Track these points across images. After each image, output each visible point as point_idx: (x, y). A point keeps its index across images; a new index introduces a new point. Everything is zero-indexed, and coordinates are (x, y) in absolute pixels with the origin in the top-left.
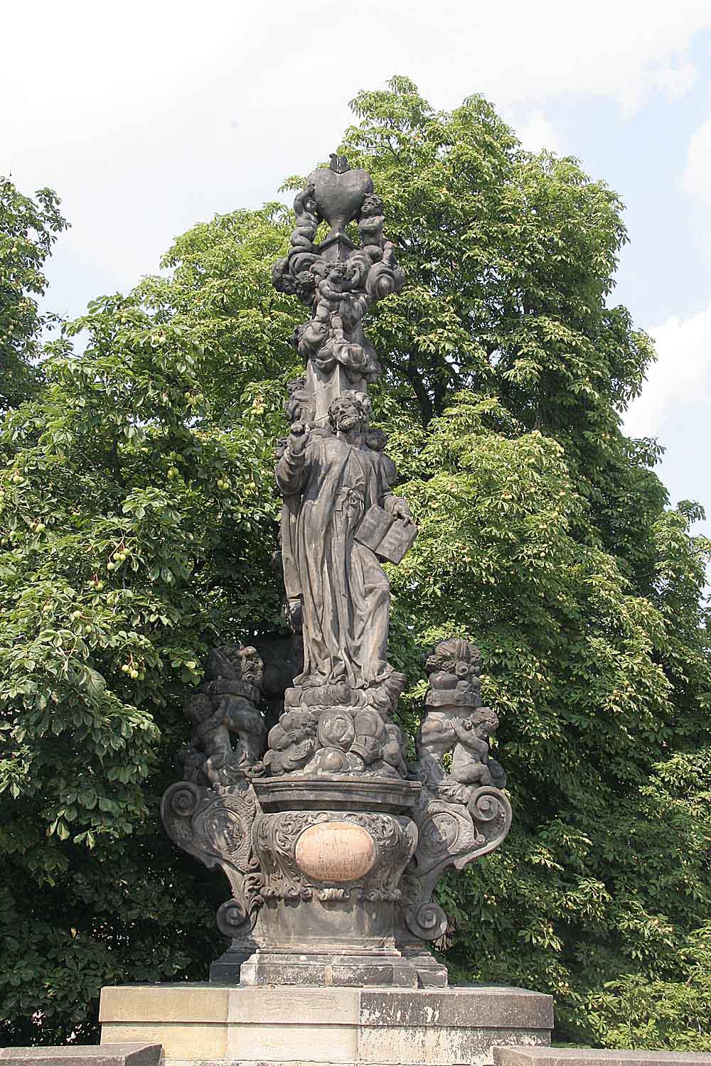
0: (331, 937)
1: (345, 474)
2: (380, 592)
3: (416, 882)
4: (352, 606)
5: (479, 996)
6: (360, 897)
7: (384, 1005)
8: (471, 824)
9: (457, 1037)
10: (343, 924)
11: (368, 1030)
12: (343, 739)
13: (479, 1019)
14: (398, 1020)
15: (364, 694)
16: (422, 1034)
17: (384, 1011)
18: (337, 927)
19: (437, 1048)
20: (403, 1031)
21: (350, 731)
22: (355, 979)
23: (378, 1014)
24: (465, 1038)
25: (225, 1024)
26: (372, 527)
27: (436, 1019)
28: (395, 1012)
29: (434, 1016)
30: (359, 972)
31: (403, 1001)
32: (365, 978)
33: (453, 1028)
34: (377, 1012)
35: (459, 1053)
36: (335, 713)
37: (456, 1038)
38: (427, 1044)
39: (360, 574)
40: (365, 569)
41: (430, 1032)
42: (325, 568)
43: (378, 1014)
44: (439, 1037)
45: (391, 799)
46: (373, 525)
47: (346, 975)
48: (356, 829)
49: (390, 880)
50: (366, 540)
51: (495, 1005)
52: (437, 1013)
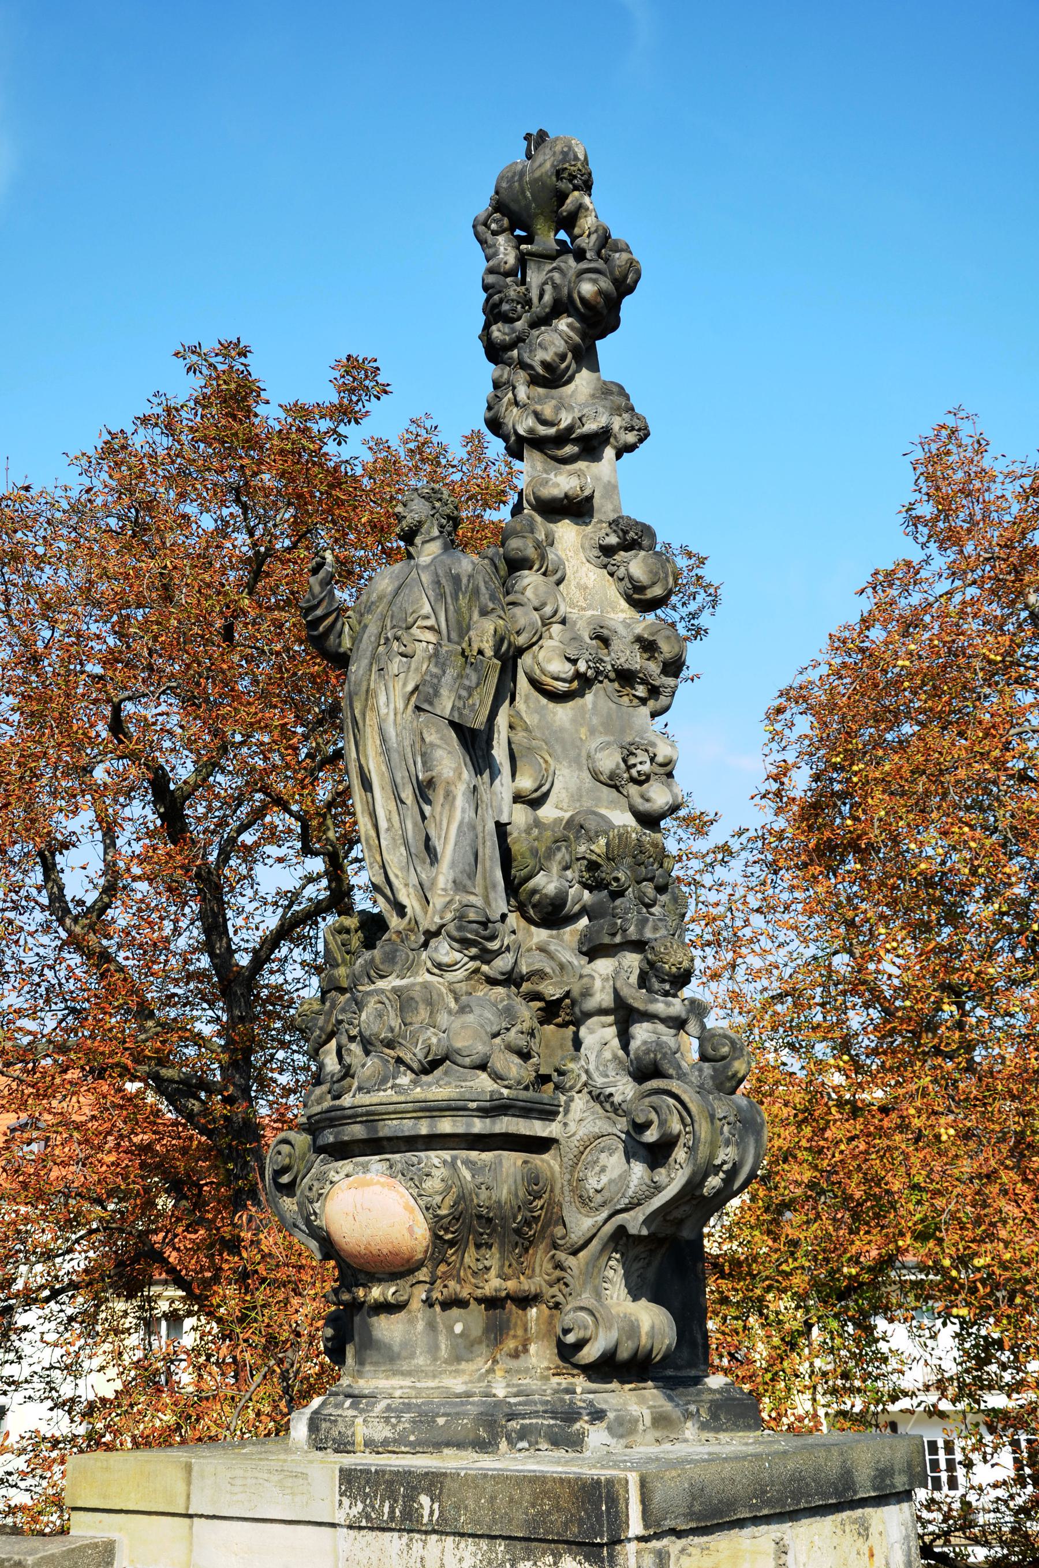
0: (388, 1367)
10: (404, 1344)
13: (494, 1521)
16: (421, 1544)
22: (395, 1441)
24: (479, 1557)
25: (191, 1516)
26: (435, 681)
28: (382, 1502)
32: (412, 1438)
33: (462, 1535)
37: (467, 1555)
48: (382, 1185)
50: (431, 703)
52: (436, 1506)
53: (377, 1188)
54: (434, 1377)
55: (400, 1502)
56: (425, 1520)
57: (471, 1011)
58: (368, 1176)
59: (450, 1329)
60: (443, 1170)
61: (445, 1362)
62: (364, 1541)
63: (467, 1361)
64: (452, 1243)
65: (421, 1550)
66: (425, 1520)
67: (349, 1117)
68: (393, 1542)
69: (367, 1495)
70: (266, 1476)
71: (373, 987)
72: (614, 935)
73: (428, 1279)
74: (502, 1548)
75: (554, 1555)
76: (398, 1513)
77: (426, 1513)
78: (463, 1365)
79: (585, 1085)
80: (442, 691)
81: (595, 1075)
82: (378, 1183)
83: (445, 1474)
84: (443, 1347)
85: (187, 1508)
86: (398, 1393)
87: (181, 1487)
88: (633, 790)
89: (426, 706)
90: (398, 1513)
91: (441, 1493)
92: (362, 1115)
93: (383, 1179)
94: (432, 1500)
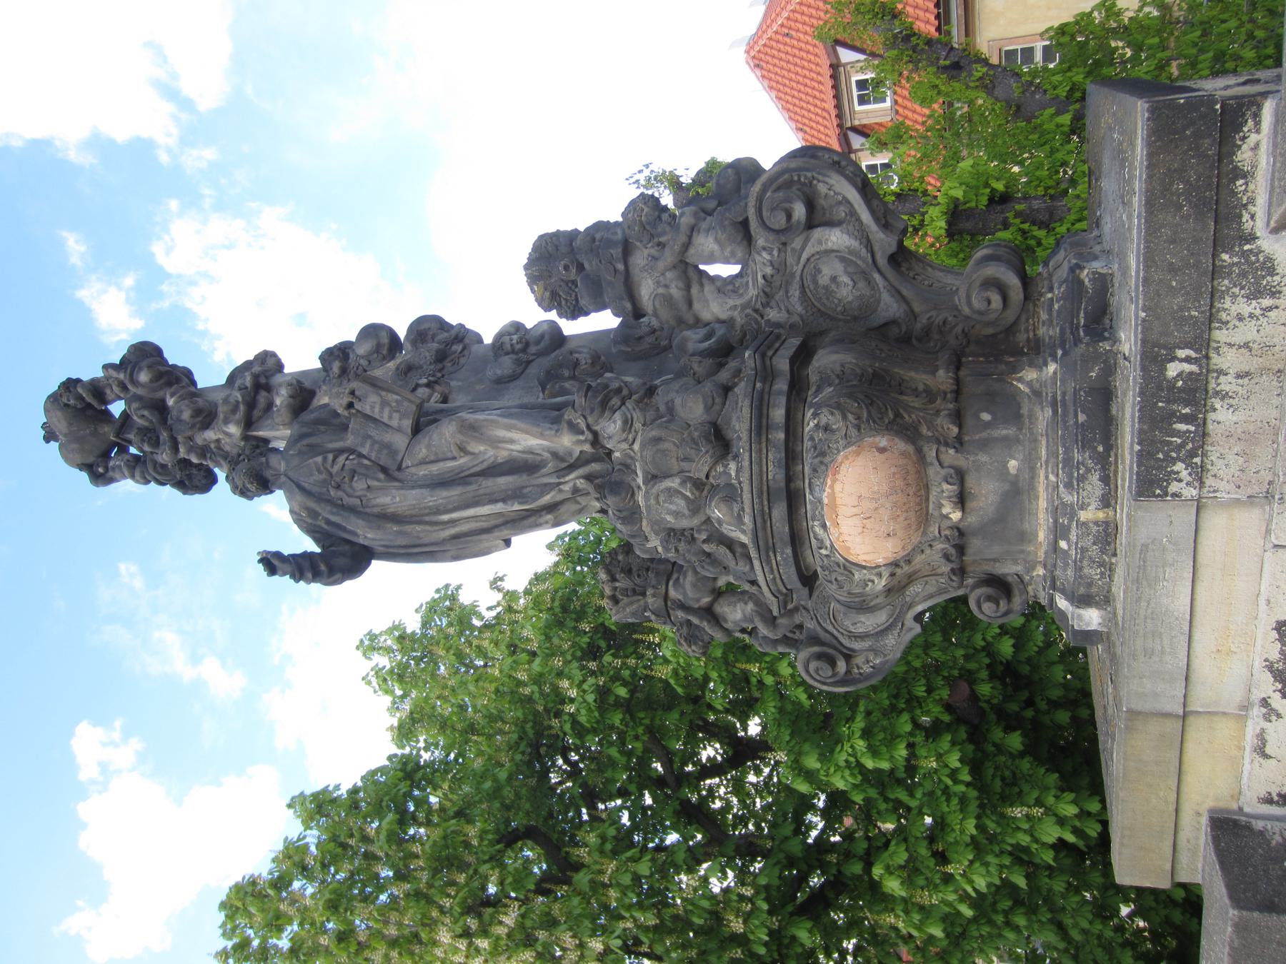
1: (315, 489)
2: (461, 437)
3: (923, 320)
4: (494, 470)
5: (1147, 268)
6: (951, 451)
7: (1161, 456)
8: (818, 233)
9: (1235, 305)
11: (1209, 481)
12: (688, 494)
13: (1197, 265)
14: (1193, 429)
15: (617, 454)
16: (1222, 379)
17: (1174, 455)
18: (1007, 487)
19: (1255, 346)
20: (1211, 416)
21: (674, 483)
22: (1104, 469)
23: (1179, 466)
24: (1236, 290)
26: (376, 446)
27: (1193, 354)
29: (1188, 360)
30: (1090, 463)
31: (1155, 422)
32: (1100, 449)
34: (1175, 468)
35: (1267, 302)
36: (648, 507)
37: (1234, 309)
38: (1245, 367)
39: (441, 465)
40: (432, 458)
41: (1216, 360)
42: (445, 517)
43: (1179, 466)
44: (1231, 345)
45: (778, 414)
46: (372, 445)
47: (1094, 485)
48: (834, 481)
49: (921, 387)
51: (1167, 232)
52: (1181, 353)
53: (838, 487)
54: (1036, 440)
55: (1175, 407)
56: (1194, 368)
57: (673, 401)
58: (826, 501)
59: (987, 425)
60: (822, 416)
61: (1020, 429)
62: (1220, 463)
63: (1020, 408)
64: (898, 415)
65: (1230, 378)
66: (1194, 368)
67: (764, 521)
68: (1222, 417)
69: (1167, 455)
70: (1143, 604)
71: (643, 509)
72: (615, 270)
73: (935, 447)
74: (1225, 257)
75: (1236, 178)
76: (1187, 410)
77: (1187, 367)
78: (1025, 411)
79: (756, 311)
80: (386, 440)
81: (747, 298)
82: (832, 487)
83: (1144, 341)
84: (1004, 432)
85: (1177, 716)
86: (1052, 478)
87: (1154, 727)
88: (533, 349)
89: (399, 458)
90: (1187, 410)
91: (1165, 347)
92: (761, 503)
93: (829, 482)
94: (1174, 359)
